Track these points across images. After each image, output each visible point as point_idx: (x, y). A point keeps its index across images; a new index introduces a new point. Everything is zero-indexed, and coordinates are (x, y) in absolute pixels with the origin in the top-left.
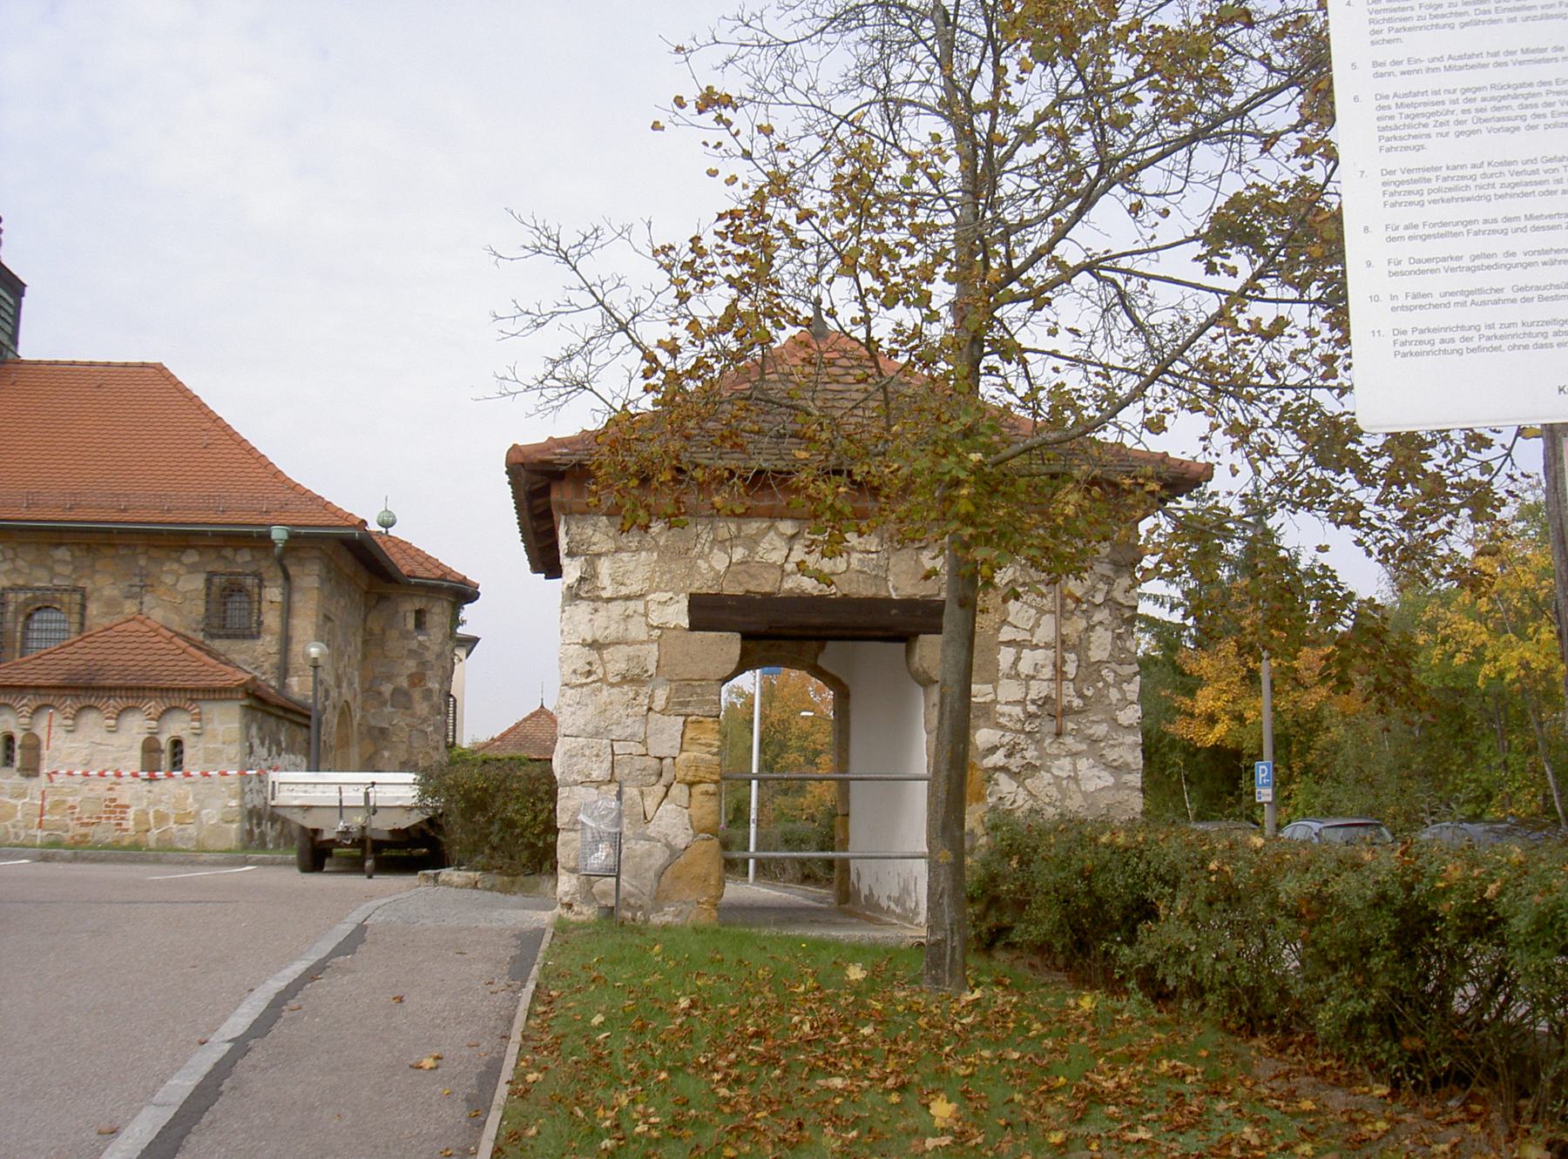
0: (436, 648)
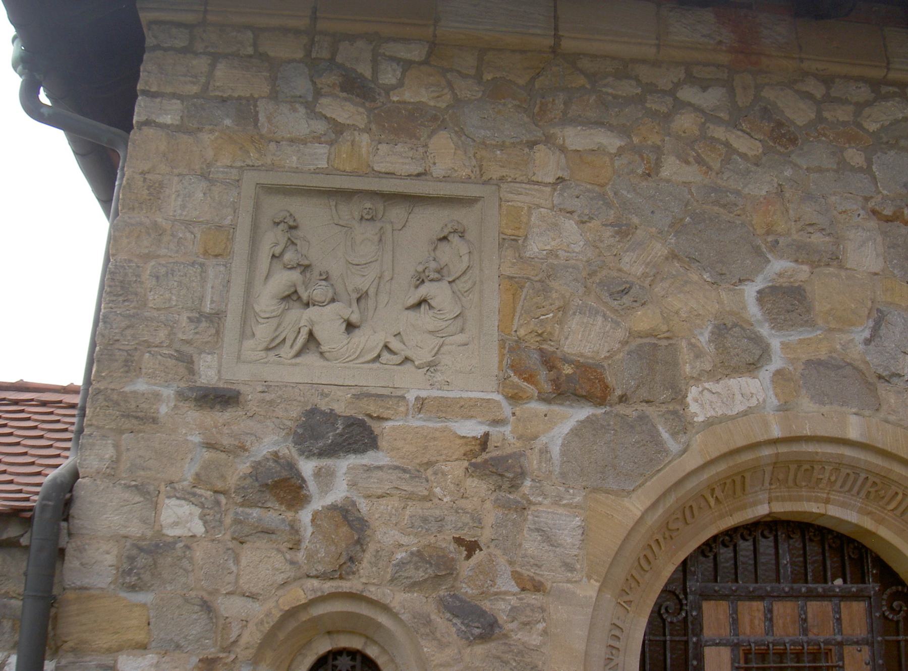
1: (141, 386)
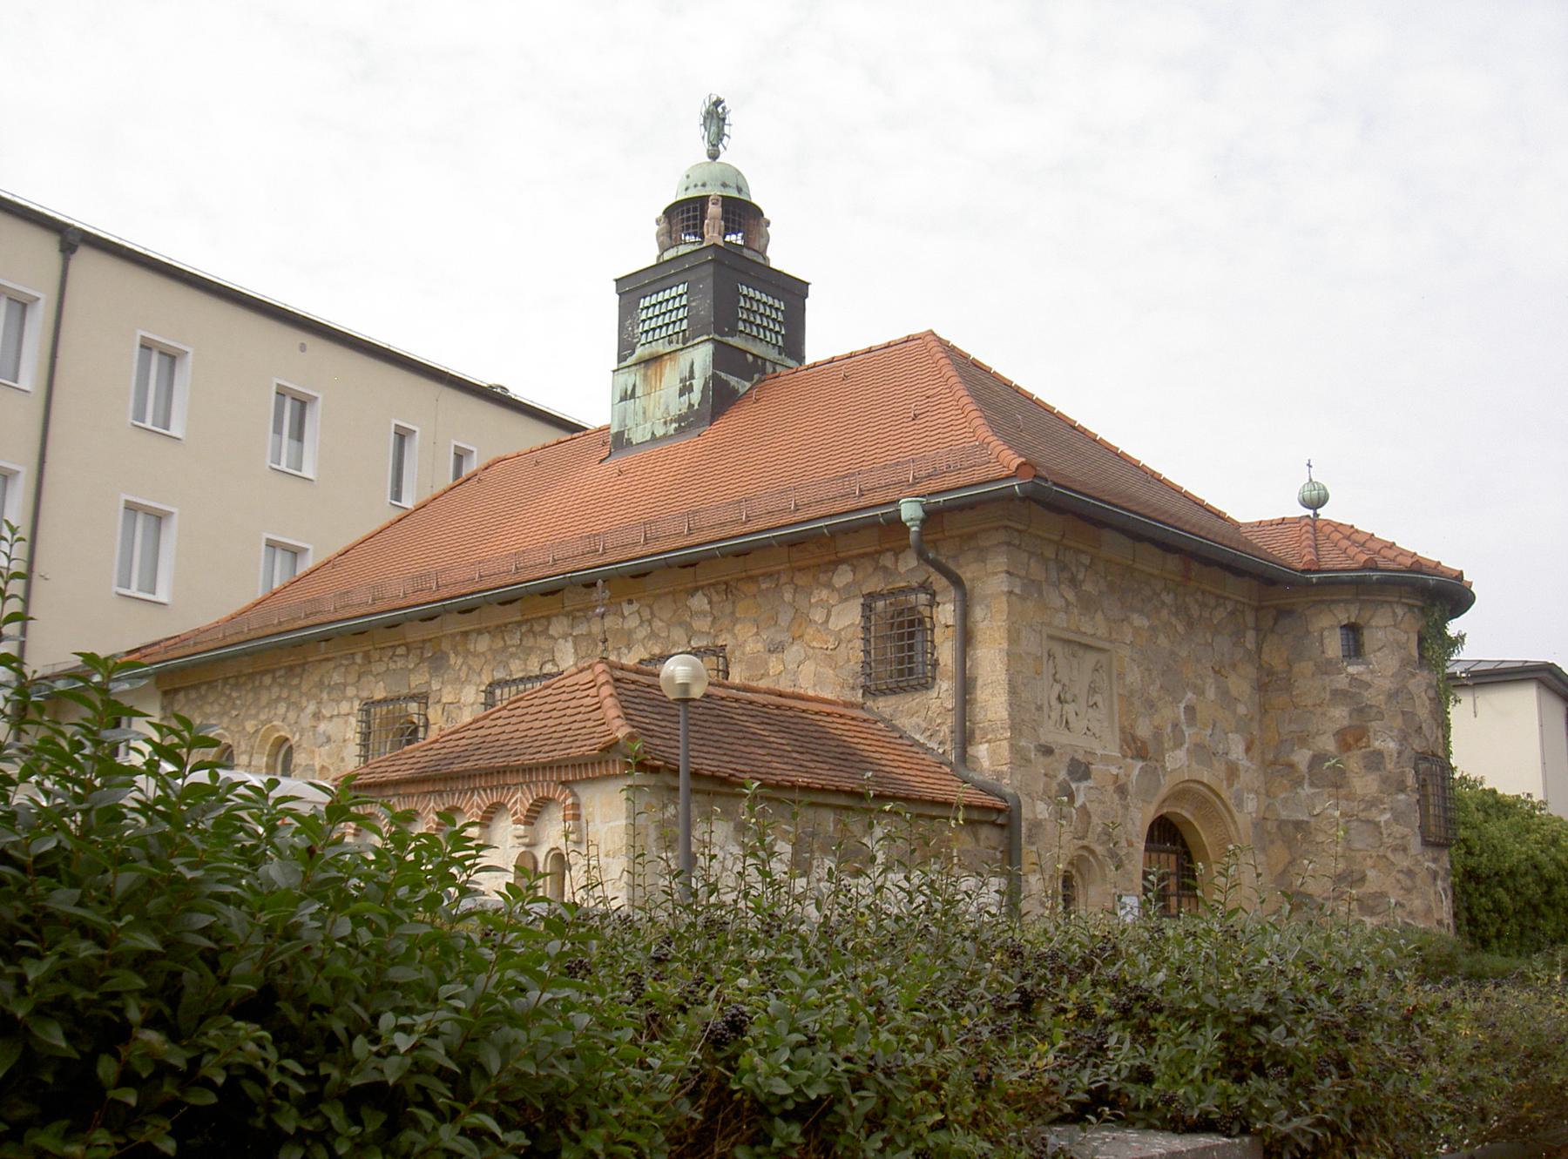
0: (1387, 684)
1: (1023, 743)
